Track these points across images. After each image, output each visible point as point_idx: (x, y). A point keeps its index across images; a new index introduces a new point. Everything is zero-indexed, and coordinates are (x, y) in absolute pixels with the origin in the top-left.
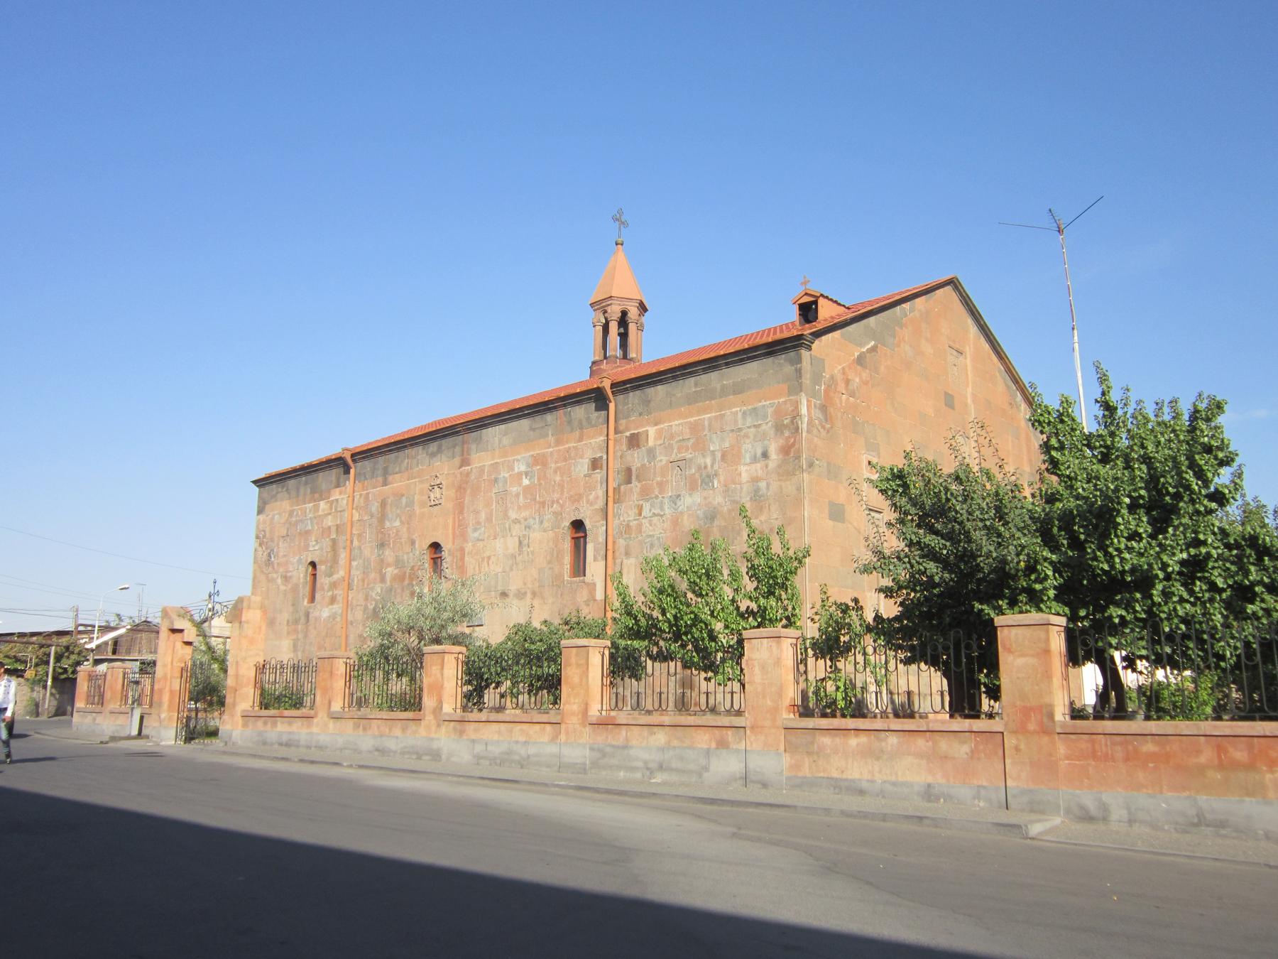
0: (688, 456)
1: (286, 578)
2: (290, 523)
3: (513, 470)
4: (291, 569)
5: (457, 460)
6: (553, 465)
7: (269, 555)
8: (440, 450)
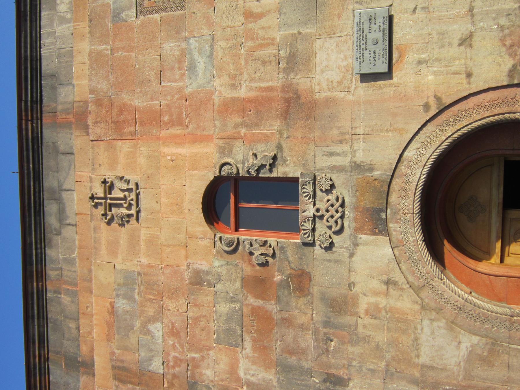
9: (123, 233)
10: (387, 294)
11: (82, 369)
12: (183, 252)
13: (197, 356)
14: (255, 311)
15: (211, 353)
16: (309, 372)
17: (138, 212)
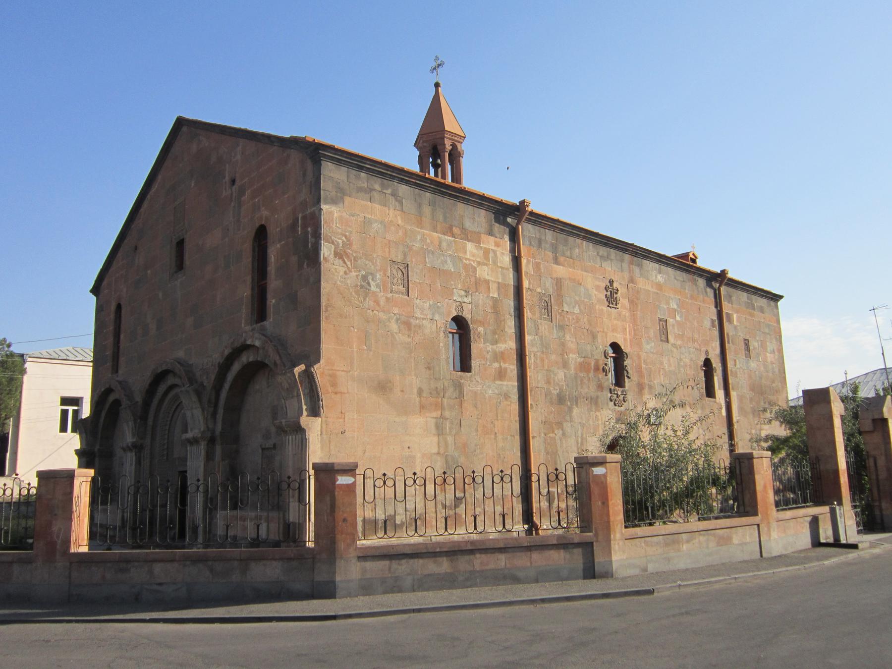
0: (749, 339)
1: (407, 325)
2: (410, 248)
3: (669, 305)
4: (418, 314)
5: (626, 275)
7: (365, 278)
8: (607, 258)
9: (602, 296)
10: (602, 424)
12: (602, 330)
14: (589, 364)
15: (575, 340)
17: (611, 307)
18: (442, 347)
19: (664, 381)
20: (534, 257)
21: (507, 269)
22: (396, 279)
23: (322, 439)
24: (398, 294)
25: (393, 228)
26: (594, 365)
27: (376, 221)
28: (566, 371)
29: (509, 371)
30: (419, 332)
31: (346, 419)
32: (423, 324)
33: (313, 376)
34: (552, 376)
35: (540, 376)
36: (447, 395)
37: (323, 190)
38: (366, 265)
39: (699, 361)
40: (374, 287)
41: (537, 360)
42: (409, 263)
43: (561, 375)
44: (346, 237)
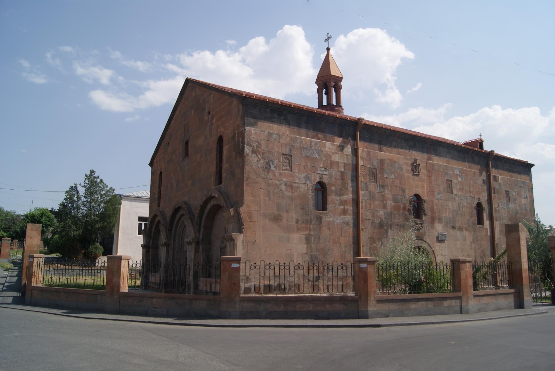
0: (509, 190)
1: (291, 186)
2: (293, 146)
3: (454, 172)
4: (297, 181)
6: (470, 176)
7: (268, 163)
9: (410, 168)
11: (379, 146)
12: (408, 187)
13: (389, 189)
15: (391, 193)
16: (391, 220)
18: (310, 198)
19: (448, 215)
20: (367, 148)
21: (350, 155)
22: (285, 163)
23: (243, 244)
24: (286, 171)
25: (284, 137)
26: (403, 207)
27: (275, 134)
28: (384, 210)
29: (349, 211)
30: (297, 190)
31: (256, 235)
32: (300, 186)
33: (239, 213)
34: (376, 213)
35: (368, 213)
36: (312, 223)
37: (246, 119)
38: (269, 156)
39: (473, 204)
40: (273, 167)
41: (366, 204)
42: (292, 154)
43: (381, 213)
44: (258, 143)
